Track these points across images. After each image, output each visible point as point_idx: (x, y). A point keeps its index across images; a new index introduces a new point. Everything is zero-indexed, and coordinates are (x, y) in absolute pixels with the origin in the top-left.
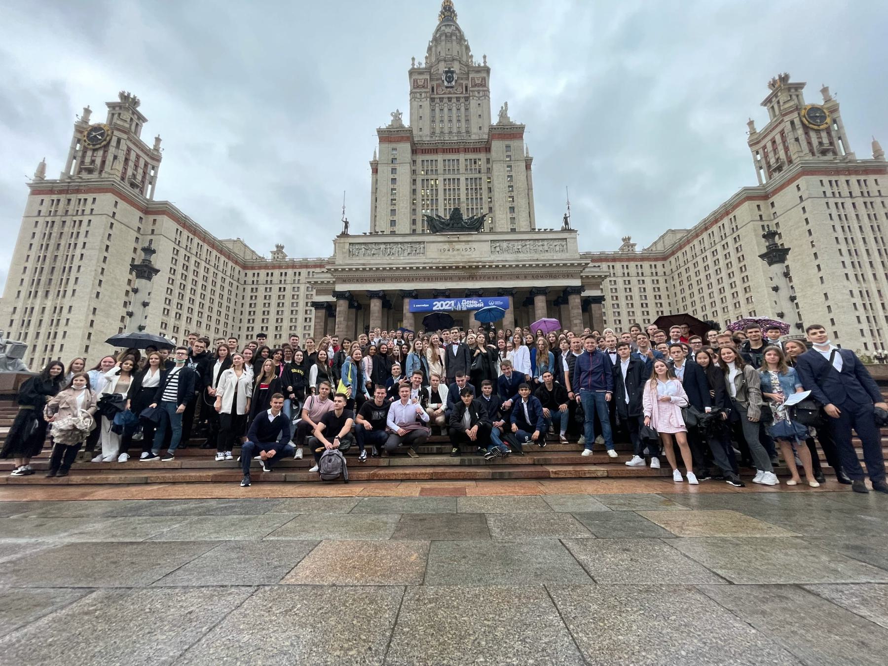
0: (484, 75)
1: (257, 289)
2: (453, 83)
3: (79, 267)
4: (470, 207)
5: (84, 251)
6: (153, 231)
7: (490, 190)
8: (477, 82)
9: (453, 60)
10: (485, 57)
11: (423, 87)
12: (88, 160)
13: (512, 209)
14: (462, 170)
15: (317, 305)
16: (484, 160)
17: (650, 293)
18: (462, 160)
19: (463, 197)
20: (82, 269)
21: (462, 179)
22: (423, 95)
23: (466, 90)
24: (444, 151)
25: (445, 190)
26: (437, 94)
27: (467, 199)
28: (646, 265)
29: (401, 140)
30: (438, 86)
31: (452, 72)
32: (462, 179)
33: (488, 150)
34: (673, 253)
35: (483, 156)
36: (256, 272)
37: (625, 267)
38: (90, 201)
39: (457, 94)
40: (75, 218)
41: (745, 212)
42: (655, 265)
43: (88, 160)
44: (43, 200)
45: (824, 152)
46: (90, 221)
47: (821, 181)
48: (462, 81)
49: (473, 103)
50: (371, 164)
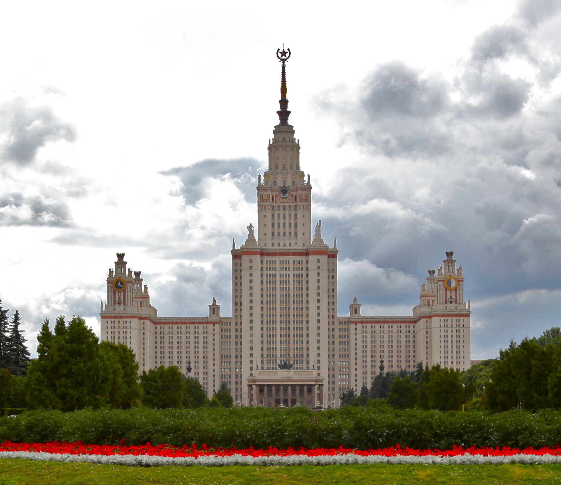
0: (307, 192)
1: (164, 337)
2: (287, 194)
4: (295, 293)
6: (144, 328)
7: (307, 282)
8: (303, 198)
9: (287, 173)
11: (267, 201)
12: (117, 298)
13: (319, 301)
14: (291, 269)
15: (248, 385)
16: (304, 262)
17: (403, 344)
18: (291, 263)
19: (291, 287)
21: (291, 276)
22: (267, 207)
23: (296, 200)
24: (281, 254)
25: (281, 282)
26: (276, 202)
28: (403, 325)
29: (254, 253)
30: (277, 196)
31: (286, 187)
32: (291, 276)
33: (307, 254)
35: (303, 259)
36: (162, 326)
37: (390, 326)
38: (128, 322)
39: (289, 203)
40: (123, 330)
41: (423, 321)
42: (409, 326)
43: (117, 298)
45: (451, 302)
46: (130, 332)
47: (440, 320)
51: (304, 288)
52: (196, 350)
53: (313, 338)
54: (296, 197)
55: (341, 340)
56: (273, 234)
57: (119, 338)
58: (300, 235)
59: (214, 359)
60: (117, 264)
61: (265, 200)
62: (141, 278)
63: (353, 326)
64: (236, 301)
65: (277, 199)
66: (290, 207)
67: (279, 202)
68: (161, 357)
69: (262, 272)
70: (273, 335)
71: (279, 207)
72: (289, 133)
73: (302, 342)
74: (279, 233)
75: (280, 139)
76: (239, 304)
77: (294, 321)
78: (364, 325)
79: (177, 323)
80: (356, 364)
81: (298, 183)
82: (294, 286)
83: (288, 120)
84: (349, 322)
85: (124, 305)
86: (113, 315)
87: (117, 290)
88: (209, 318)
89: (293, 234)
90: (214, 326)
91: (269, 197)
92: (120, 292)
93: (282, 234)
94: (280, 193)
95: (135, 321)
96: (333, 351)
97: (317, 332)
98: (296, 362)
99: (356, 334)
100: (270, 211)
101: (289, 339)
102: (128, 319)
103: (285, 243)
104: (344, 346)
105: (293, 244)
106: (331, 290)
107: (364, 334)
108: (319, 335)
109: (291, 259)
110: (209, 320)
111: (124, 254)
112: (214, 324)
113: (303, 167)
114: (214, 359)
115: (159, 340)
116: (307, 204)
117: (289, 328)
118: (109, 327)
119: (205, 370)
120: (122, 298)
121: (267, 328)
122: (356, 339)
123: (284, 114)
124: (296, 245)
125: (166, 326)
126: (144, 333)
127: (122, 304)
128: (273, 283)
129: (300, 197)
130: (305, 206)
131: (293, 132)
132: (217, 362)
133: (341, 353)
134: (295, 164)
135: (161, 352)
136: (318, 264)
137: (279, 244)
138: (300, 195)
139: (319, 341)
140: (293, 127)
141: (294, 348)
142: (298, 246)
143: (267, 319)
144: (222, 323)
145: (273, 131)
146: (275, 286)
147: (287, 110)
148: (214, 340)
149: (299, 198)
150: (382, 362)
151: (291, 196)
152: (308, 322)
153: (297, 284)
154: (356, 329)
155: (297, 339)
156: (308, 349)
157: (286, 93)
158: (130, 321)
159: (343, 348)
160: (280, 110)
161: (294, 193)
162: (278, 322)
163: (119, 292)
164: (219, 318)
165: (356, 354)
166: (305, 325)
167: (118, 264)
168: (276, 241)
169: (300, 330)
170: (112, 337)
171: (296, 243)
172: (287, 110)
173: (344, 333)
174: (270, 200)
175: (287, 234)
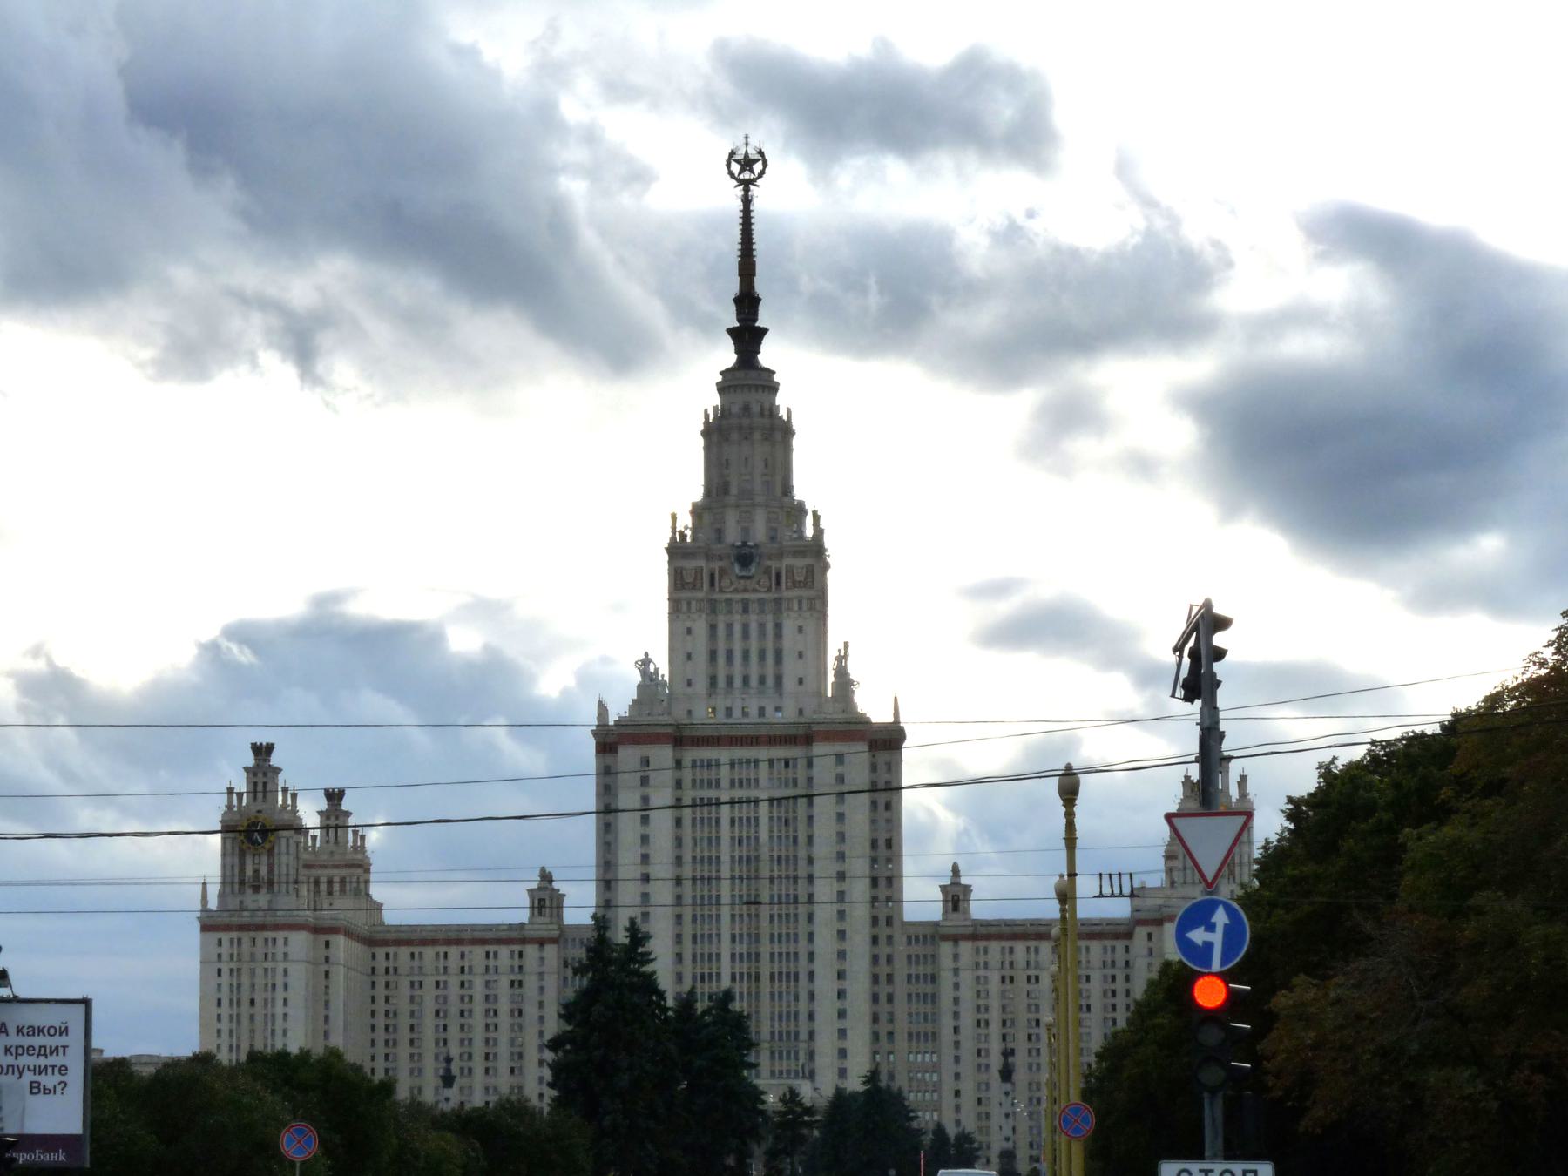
2: (753, 569)
4: (775, 854)
7: (810, 818)
8: (798, 579)
11: (694, 587)
12: (249, 872)
16: (802, 763)
19: (764, 835)
20: (289, 1034)
22: (694, 603)
26: (721, 591)
27: (771, 838)
31: (751, 547)
33: (808, 740)
36: (391, 950)
40: (266, 965)
42: (1113, 949)
43: (249, 872)
44: (220, 942)
48: (769, 563)
49: (789, 627)
50: (595, 734)
51: (802, 839)
52: (489, 1021)
53: (825, 985)
54: (778, 576)
55: (913, 988)
56: (713, 681)
57: (253, 986)
58: (789, 684)
60: (251, 776)
61: (688, 583)
62: (344, 808)
63: (946, 948)
65: (726, 582)
66: (761, 602)
67: (731, 589)
68: (387, 1042)
69: (679, 792)
70: (710, 975)
71: (729, 602)
72: (760, 391)
73: (797, 998)
74: (730, 681)
75: (735, 409)
77: (772, 935)
78: (981, 944)
79: (433, 942)
80: (957, 1059)
81: (787, 536)
82: (771, 831)
83: (759, 352)
84: (937, 939)
85: (268, 892)
86: (235, 920)
87: (249, 848)
88: (527, 927)
89: (770, 681)
91: (699, 575)
92: (259, 855)
93: (738, 682)
94: (732, 563)
95: (299, 942)
96: (891, 1021)
97: (837, 966)
98: (777, 1055)
99: (956, 971)
100: (704, 616)
101: (758, 987)
103: (748, 708)
104: (922, 1009)
105: (769, 710)
106: (882, 843)
107: (981, 973)
108: (841, 975)
109: (763, 753)
110: (528, 934)
111: (272, 745)
113: (806, 485)
115: (381, 991)
116: (811, 593)
117: (758, 955)
118: (225, 957)
120: (264, 871)
121: (694, 956)
122: (957, 986)
123: (747, 337)
124: (780, 715)
125: (404, 952)
126: (327, 974)
127: (264, 890)
128: (710, 824)
131: (774, 388)
133: (914, 1028)
134: (778, 479)
135: (387, 1028)
136: (840, 770)
137: (729, 712)
138: (790, 570)
139: (841, 994)
140: (774, 373)
141: (773, 1013)
142: (785, 715)
143: (694, 929)
144: (566, 941)
145: (718, 384)
146: (717, 832)
147: (757, 324)
148: (542, 989)
149: (787, 578)
150: (1008, 1053)
151: (765, 573)
152: (811, 937)
153: (779, 826)
154: (956, 957)
155: (780, 987)
156: (811, 1016)
157: (754, 275)
158: (286, 939)
159: (917, 1014)
160: (737, 324)
161: (774, 564)
162: (726, 937)
163: (254, 855)
164: (555, 927)
165: (956, 1030)
166: (803, 947)
167: (255, 775)
168: (721, 702)
169: (788, 960)
170: (231, 985)
171: (778, 709)
172: (757, 324)
173: (921, 970)
174: (702, 583)
175: (754, 681)
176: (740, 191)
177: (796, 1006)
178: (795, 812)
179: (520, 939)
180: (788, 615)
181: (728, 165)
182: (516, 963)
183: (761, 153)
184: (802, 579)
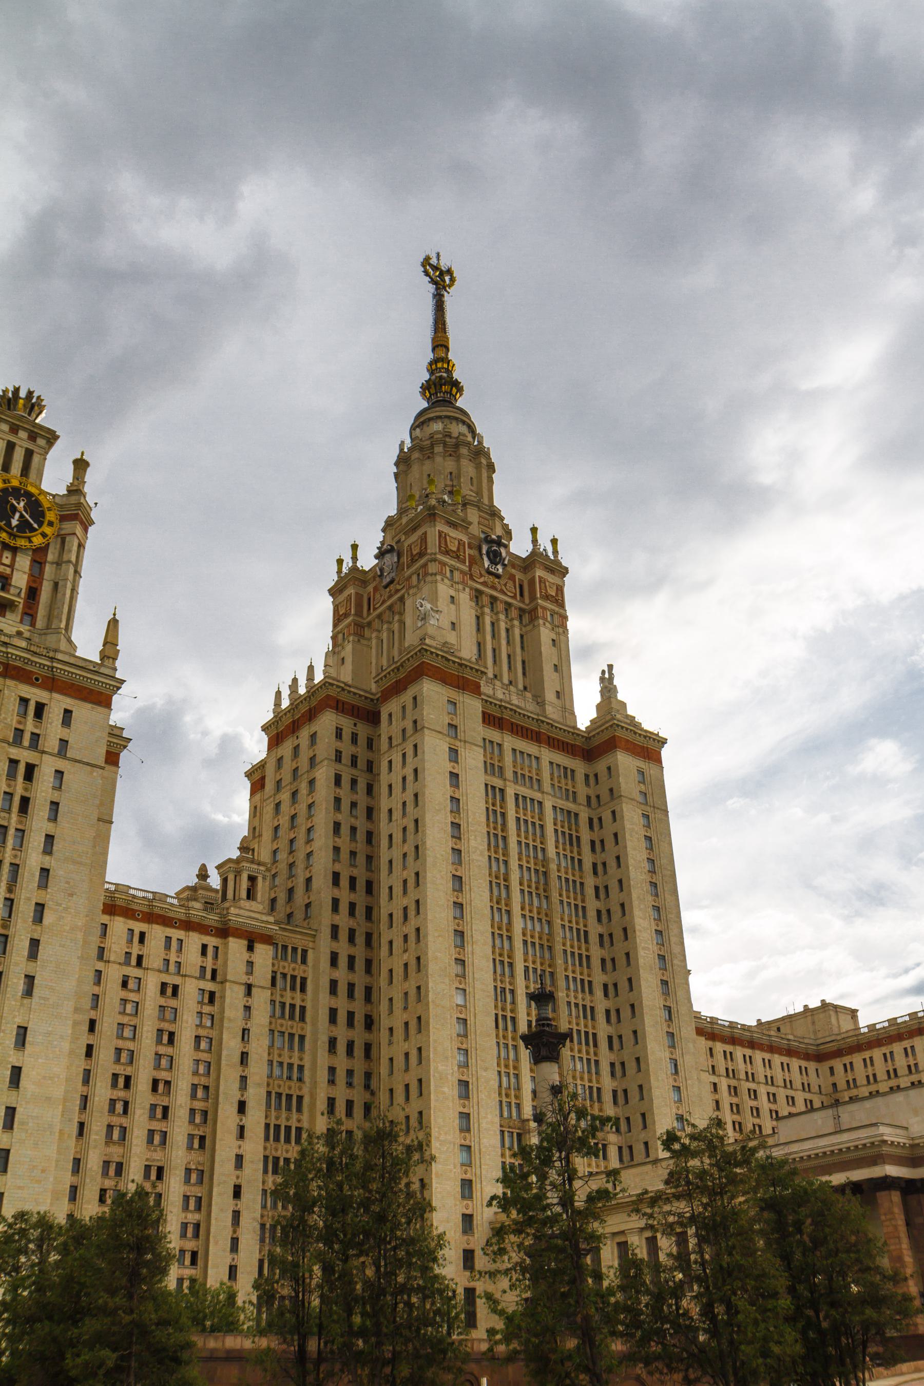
3: (40, 908)
5: (47, 861)
10: (554, 542)
11: (458, 557)
16: (579, 777)
19: (551, 851)
20: (48, 918)
22: (456, 574)
23: (522, 594)
25: (518, 819)
27: (558, 854)
28: (795, 1063)
34: (838, 1053)
35: (579, 766)
39: (506, 594)
40: (15, 752)
46: (59, 773)
48: (513, 571)
49: (546, 634)
52: (162, 1050)
54: (521, 587)
59: (242, 1107)
64: (337, 867)
65: (476, 570)
66: (508, 605)
67: (482, 580)
76: (344, 882)
90: (250, 948)
91: (462, 550)
102: (56, 696)
109: (547, 755)
112: (252, 940)
114: (242, 1107)
116: (561, 611)
119: (196, 1158)
129: (543, 585)
130: (556, 616)
132: (255, 1118)
149: (540, 588)
151: (509, 579)
176: (431, 288)
177: (598, 1082)
178: (577, 831)
179: (217, 928)
180: (544, 624)
181: (423, 265)
182: (209, 964)
183: (449, 272)
184: (554, 594)
